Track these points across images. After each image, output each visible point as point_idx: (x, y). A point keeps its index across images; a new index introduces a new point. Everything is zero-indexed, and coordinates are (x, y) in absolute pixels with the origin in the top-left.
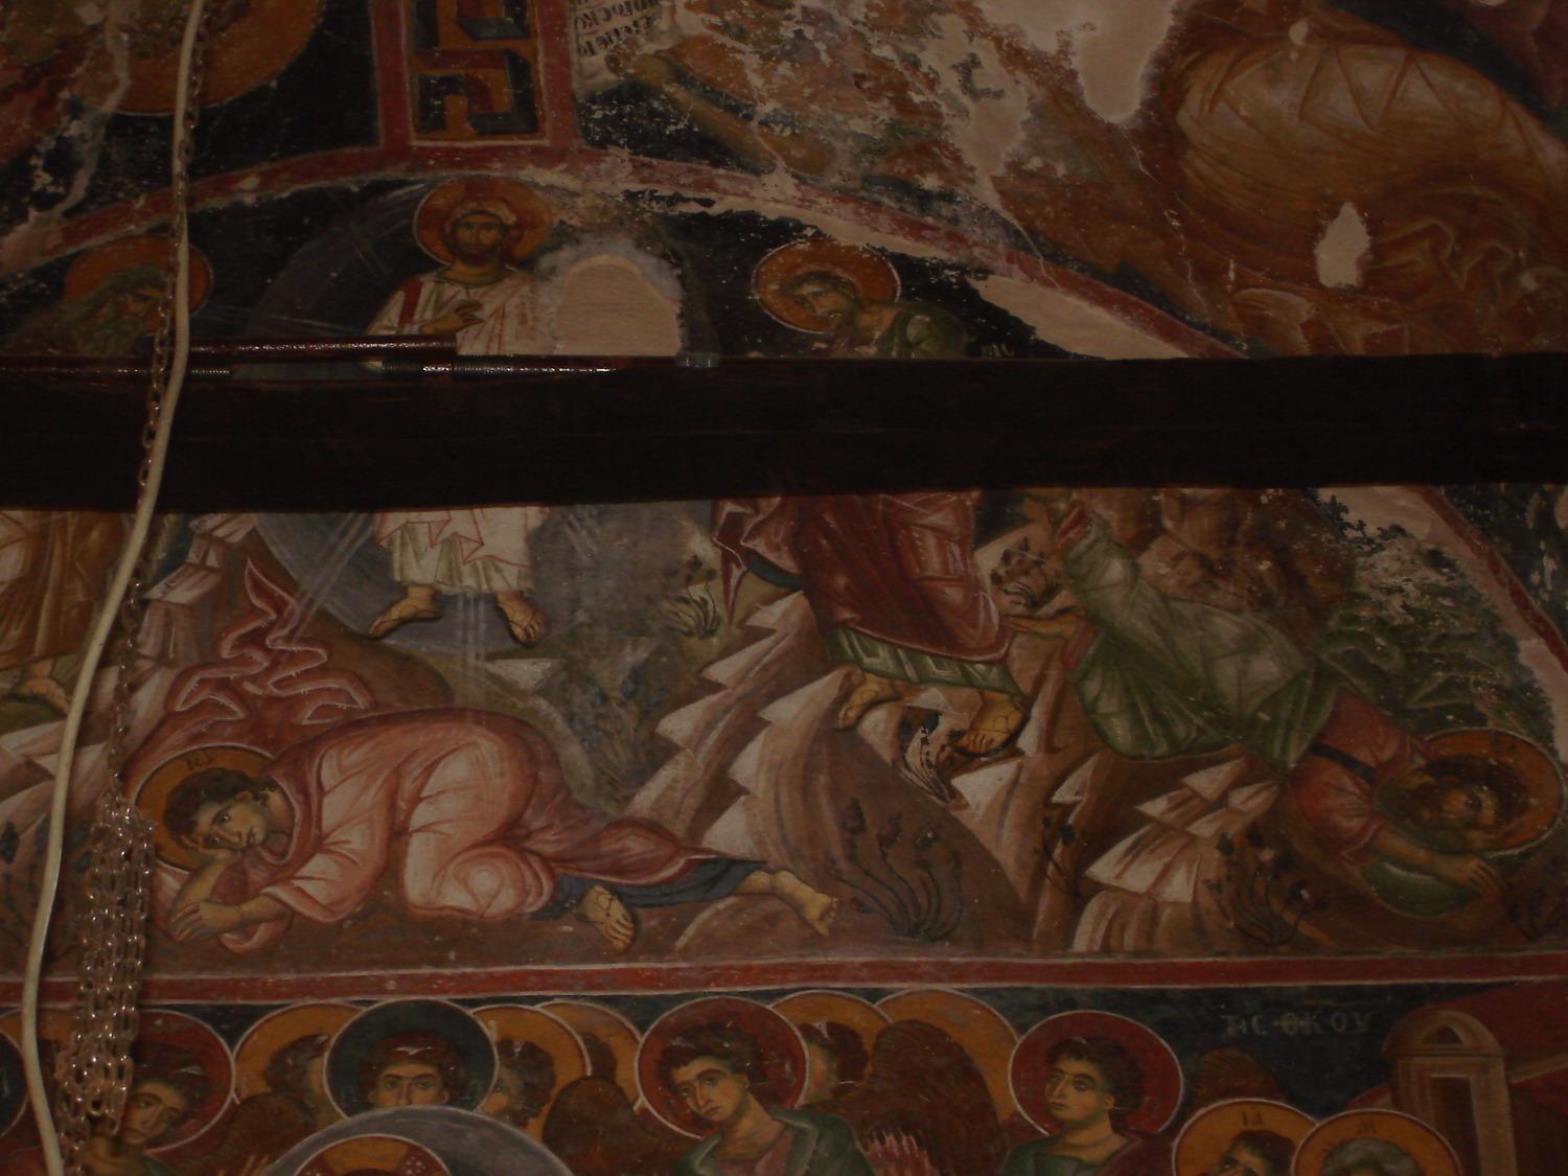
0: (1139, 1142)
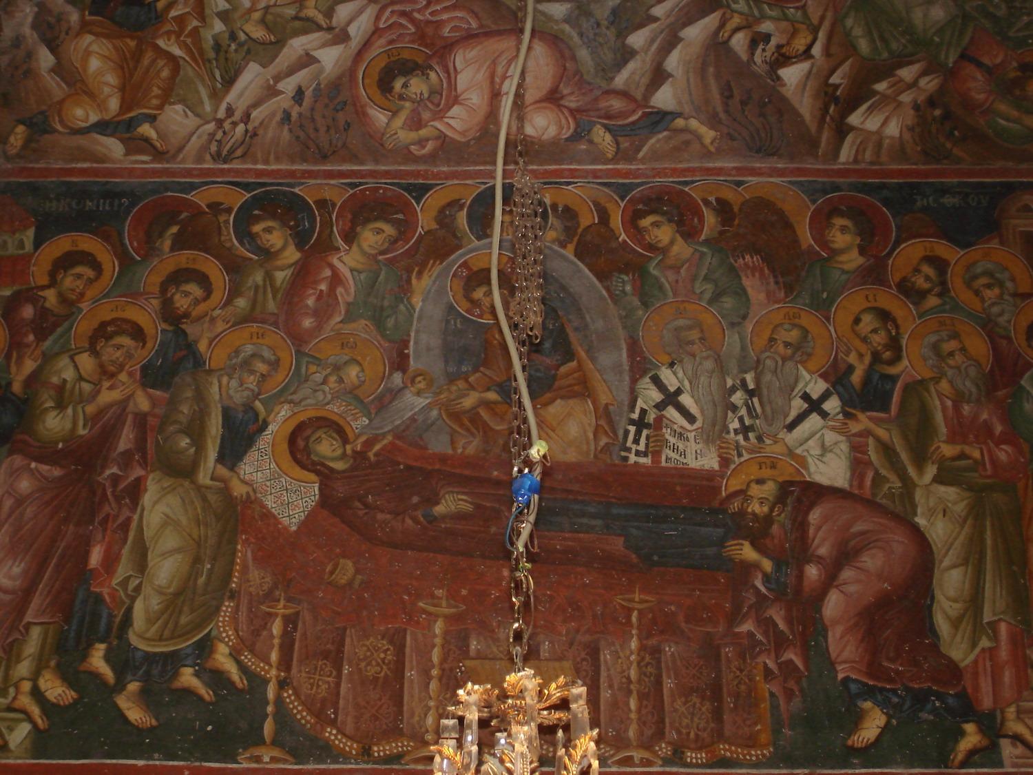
0: (872, 260)
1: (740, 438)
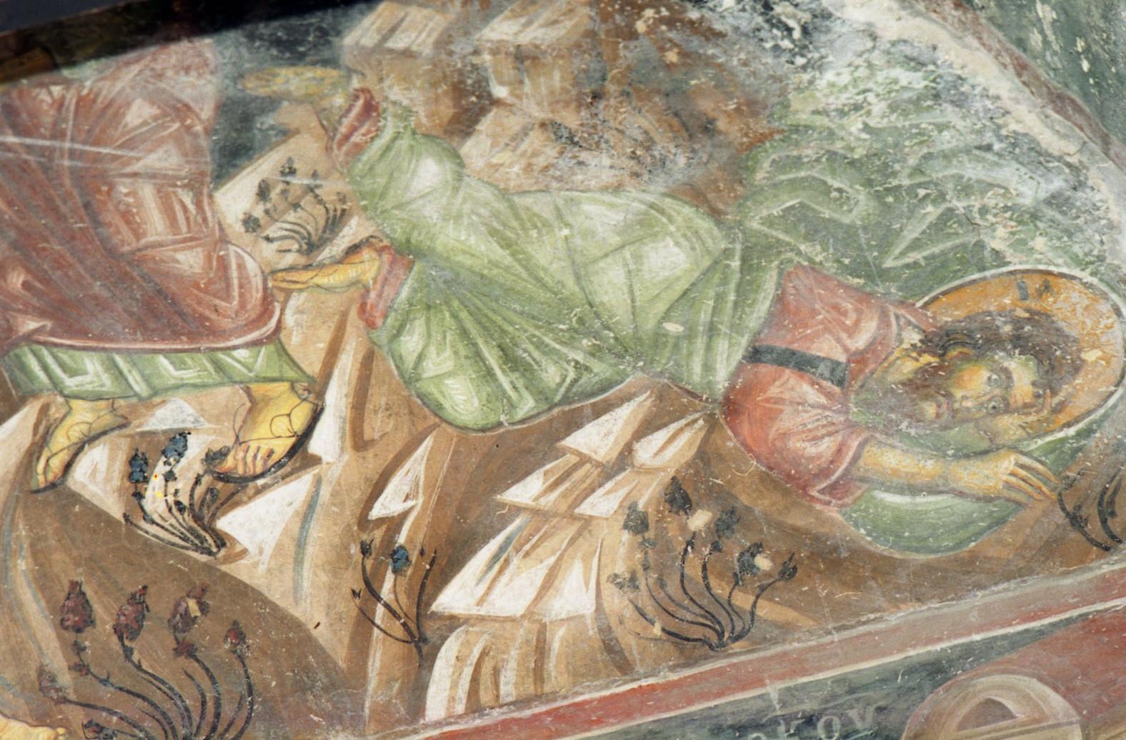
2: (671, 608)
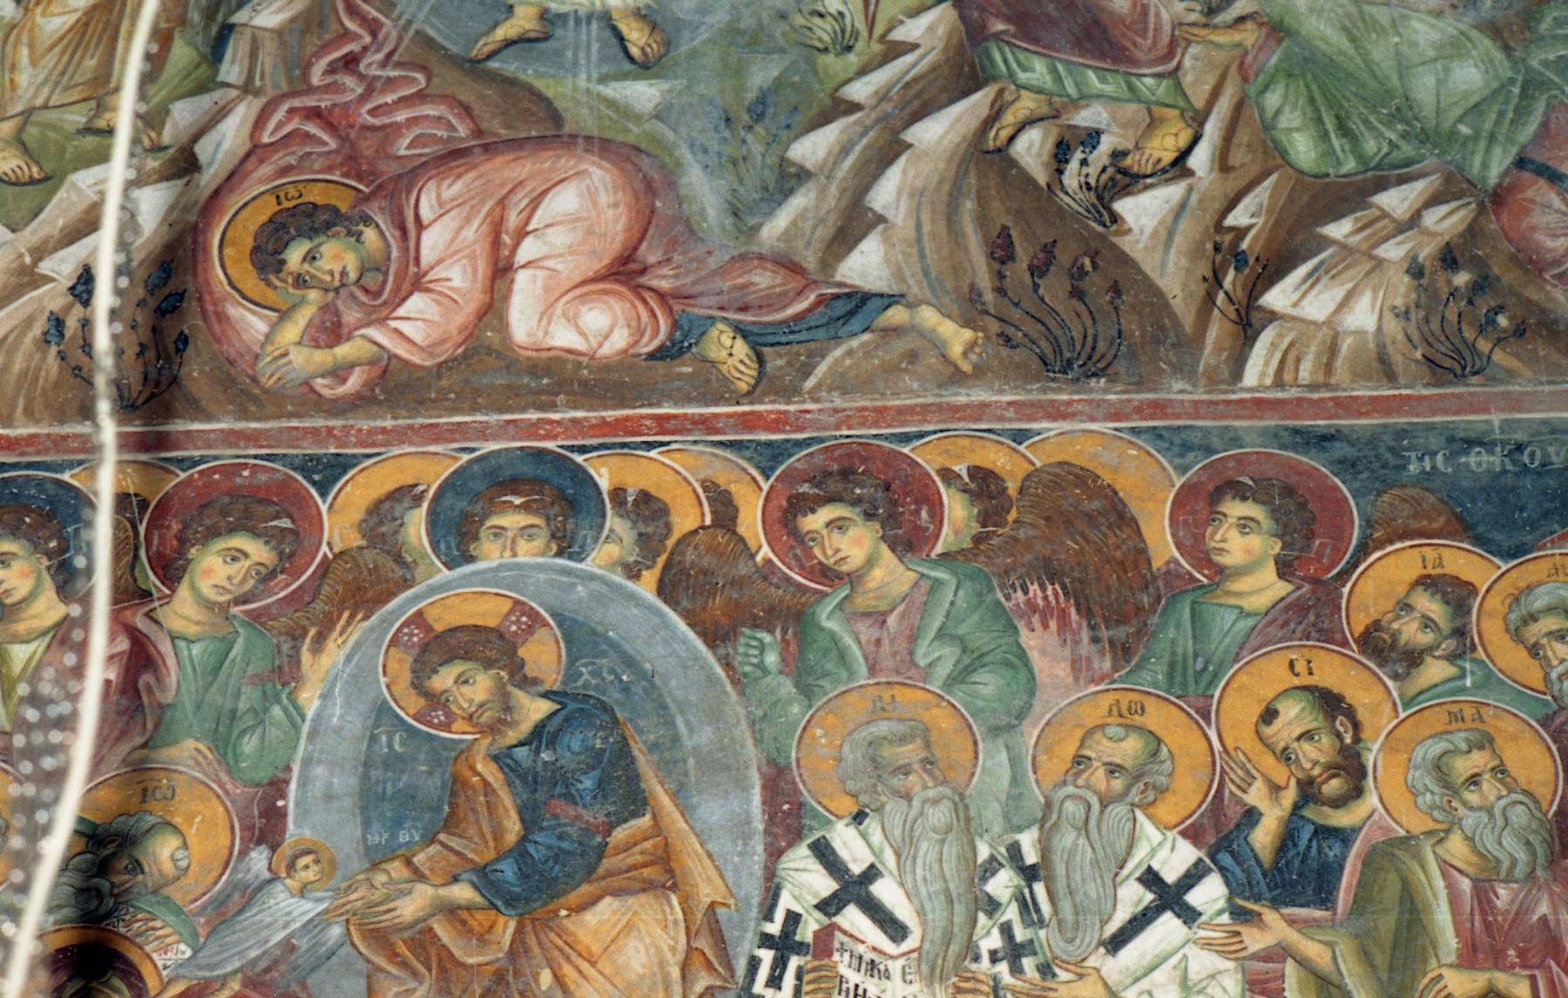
0: (1307, 588)
1: (1003, 968)
2: (1431, 340)
